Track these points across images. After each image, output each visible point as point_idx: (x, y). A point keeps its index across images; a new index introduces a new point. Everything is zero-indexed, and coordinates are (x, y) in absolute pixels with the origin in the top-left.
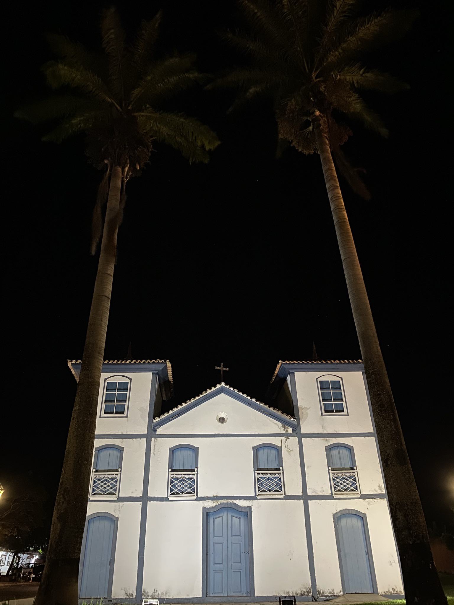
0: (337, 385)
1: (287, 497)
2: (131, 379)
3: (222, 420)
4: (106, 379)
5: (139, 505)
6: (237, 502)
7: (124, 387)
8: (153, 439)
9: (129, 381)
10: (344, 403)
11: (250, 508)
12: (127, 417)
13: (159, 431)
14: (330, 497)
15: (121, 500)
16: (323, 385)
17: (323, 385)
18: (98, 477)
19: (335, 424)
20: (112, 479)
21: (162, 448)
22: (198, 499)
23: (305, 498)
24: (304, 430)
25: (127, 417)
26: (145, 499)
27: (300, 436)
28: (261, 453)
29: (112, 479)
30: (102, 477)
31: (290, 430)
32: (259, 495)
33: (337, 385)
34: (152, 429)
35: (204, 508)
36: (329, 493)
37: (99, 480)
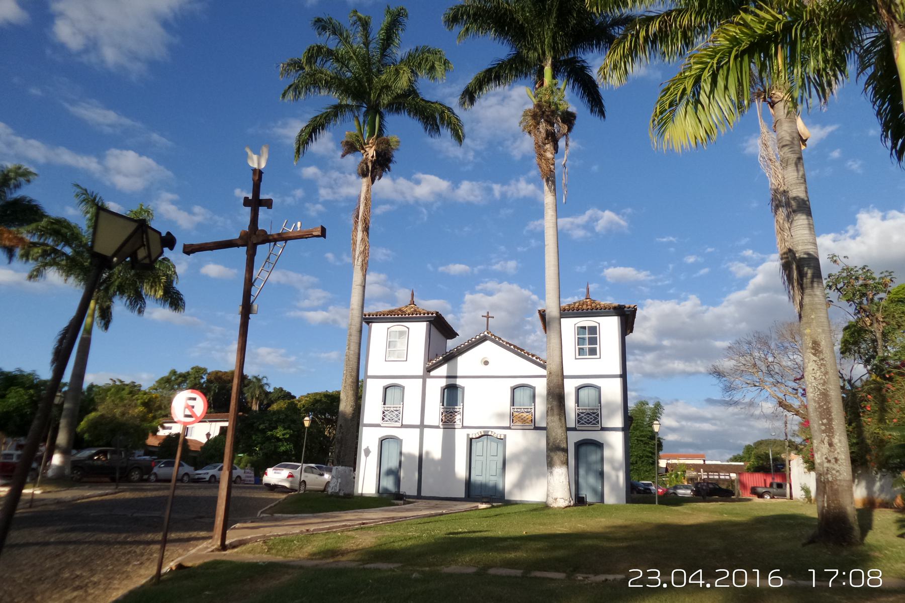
0: (593, 330)
1: (536, 428)
8: (428, 380)
10: (598, 346)
11: (505, 436)
13: (432, 373)
14: (574, 429)
15: (403, 426)
19: (588, 366)
22: (463, 427)
26: (422, 426)
33: (593, 330)
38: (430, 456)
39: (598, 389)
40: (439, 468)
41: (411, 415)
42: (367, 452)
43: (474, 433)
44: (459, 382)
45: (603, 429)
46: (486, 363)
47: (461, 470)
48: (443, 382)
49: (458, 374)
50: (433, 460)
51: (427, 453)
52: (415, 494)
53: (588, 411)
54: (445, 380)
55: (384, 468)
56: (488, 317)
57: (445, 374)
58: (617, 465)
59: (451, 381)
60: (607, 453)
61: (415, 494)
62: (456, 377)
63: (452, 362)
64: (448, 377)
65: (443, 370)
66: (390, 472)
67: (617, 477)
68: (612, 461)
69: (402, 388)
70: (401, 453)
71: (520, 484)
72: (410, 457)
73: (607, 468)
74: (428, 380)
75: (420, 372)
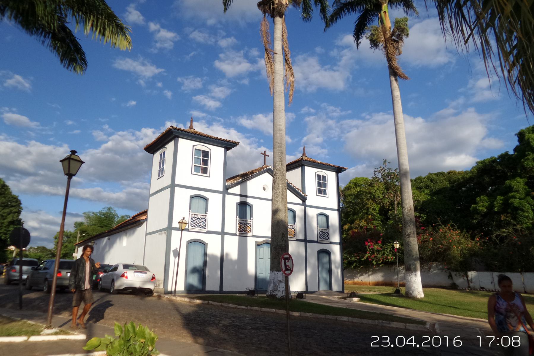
0: (324, 178)
4: (193, 146)
13: (230, 191)
14: (317, 242)
16: (319, 177)
17: (319, 177)
18: (193, 216)
20: (203, 218)
21: (233, 201)
22: (253, 236)
23: (305, 241)
24: (307, 202)
27: (306, 206)
29: (203, 218)
30: (196, 216)
31: (300, 202)
33: (324, 178)
34: (226, 188)
35: (256, 242)
36: (316, 240)
38: (229, 258)
39: (327, 217)
40: (236, 267)
41: (213, 223)
43: (260, 240)
44: (249, 200)
45: (331, 243)
46: (264, 189)
47: (251, 268)
48: (238, 199)
49: (248, 195)
50: (231, 260)
51: (227, 255)
52: (218, 290)
53: (324, 231)
54: (239, 197)
55: (191, 267)
56: (265, 155)
57: (239, 193)
58: (337, 265)
59: (244, 199)
60: (333, 257)
61: (218, 290)
62: (246, 196)
63: (243, 184)
64: (241, 196)
65: (237, 190)
66: (195, 270)
67: (338, 273)
68: (335, 262)
69: (206, 200)
70: (205, 254)
72: (214, 257)
73: (333, 267)
75: (221, 189)
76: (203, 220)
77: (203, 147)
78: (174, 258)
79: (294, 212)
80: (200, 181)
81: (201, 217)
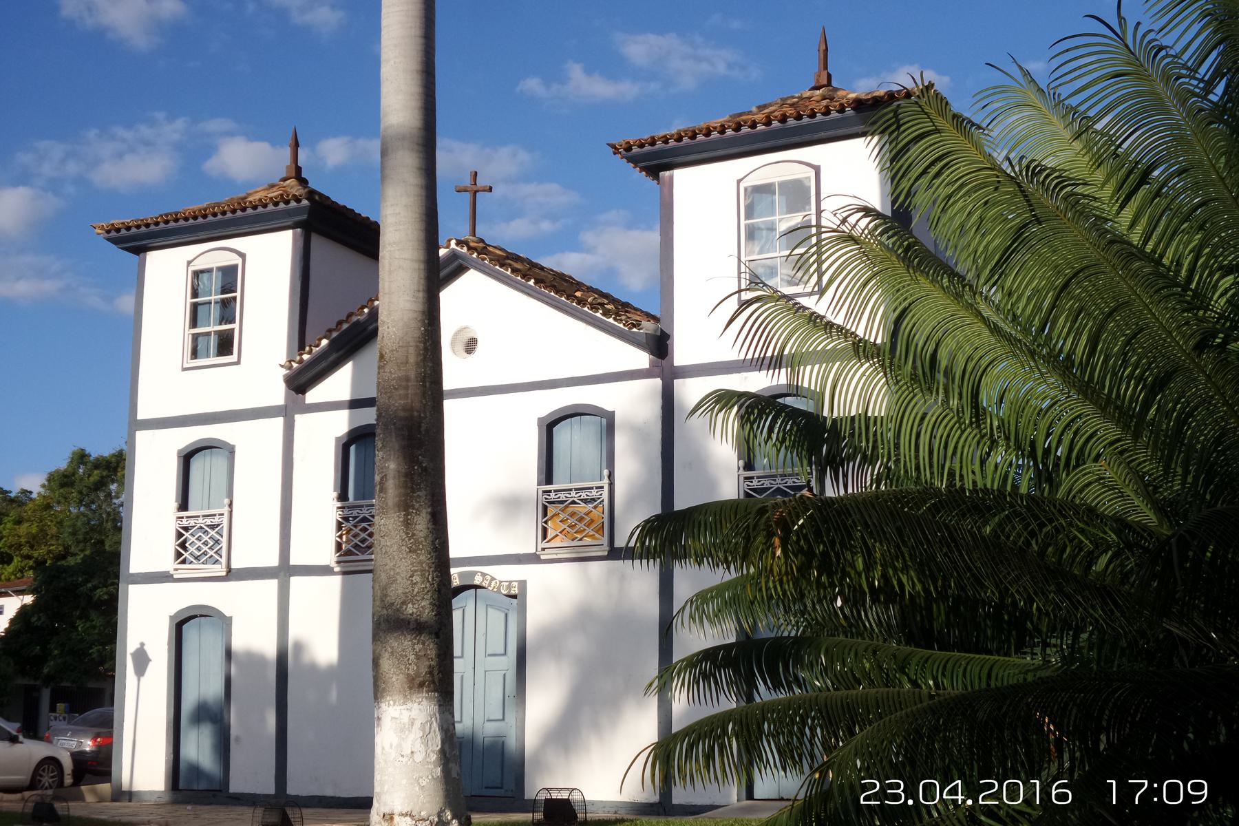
2: (243, 256)
3: (471, 345)
5: (272, 585)
6: (490, 570)
7: (230, 278)
8: (300, 419)
9: (239, 261)
11: (523, 585)
12: (238, 363)
13: (312, 396)
15: (232, 574)
18: (185, 523)
20: (212, 527)
24: (682, 355)
25: (238, 363)
26: (284, 571)
28: (562, 434)
32: (544, 549)
37: (186, 529)
38: (306, 658)
40: (334, 695)
42: (142, 661)
50: (313, 668)
51: (299, 647)
54: (344, 414)
57: (346, 395)
69: (229, 451)
70: (229, 654)
71: (567, 732)
72: (253, 660)
74: (300, 419)
75: (277, 394)
76: (212, 533)
77: (211, 255)
78: (135, 678)
79: (608, 423)
80: (217, 386)
81: (208, 521)
